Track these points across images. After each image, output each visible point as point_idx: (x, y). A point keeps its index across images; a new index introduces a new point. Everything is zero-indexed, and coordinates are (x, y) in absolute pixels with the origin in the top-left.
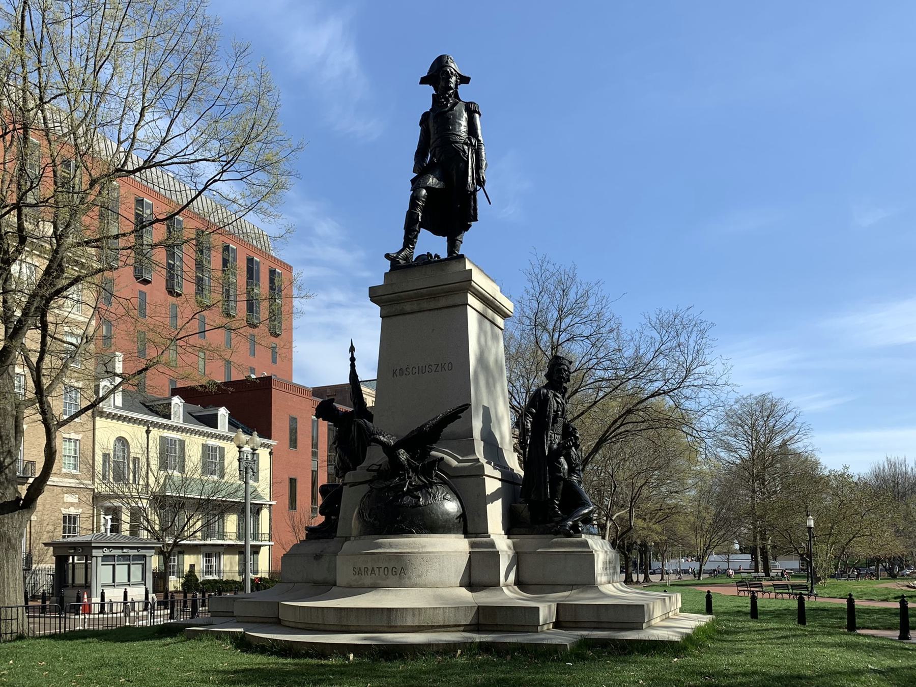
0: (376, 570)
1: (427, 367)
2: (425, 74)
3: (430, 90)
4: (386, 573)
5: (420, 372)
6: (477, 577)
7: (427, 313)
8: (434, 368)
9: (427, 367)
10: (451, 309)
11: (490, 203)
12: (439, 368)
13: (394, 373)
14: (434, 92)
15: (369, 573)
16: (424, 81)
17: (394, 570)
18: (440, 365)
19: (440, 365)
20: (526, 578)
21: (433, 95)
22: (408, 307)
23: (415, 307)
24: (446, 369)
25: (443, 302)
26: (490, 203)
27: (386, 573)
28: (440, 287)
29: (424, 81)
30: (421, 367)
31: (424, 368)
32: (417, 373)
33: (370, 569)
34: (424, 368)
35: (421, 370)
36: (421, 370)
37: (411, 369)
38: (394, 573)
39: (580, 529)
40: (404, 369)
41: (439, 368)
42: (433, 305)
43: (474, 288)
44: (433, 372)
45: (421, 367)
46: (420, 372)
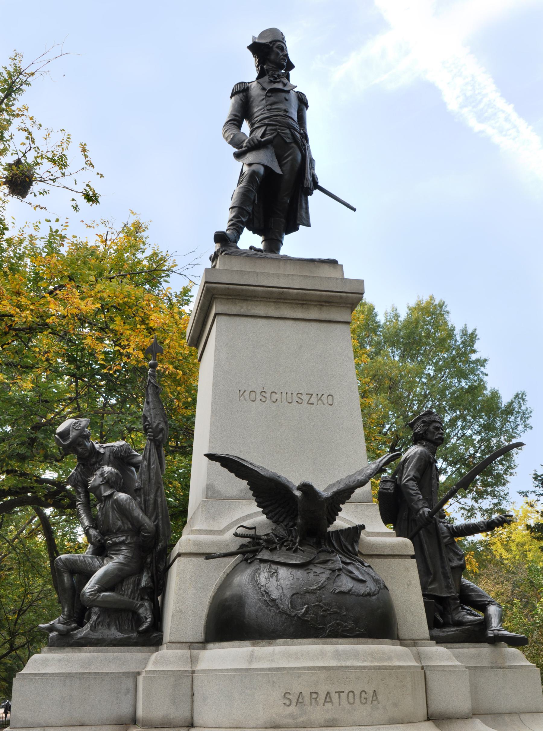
0: (335, 697)
1: (295, 395)
5: (284, 401)
7: (291, 322)
9: (295, 395)
10: (326, 325)
11: (354, 210)
12: (313, 400)
13: (242, 394)
18: (315, 395)
19: (315, 395)
22: (261, 310)
24: (325, 402)
26: (354, 210)
27: (351, 700)
30: (284, 394)
31: (289, 395)
33: (323, 696)
34: (289, 395)
37: (268, 395)
38: (364, 701)
40: (258, 392)
41: (313, 400)
42: (299, 314)
45: (284, 394)
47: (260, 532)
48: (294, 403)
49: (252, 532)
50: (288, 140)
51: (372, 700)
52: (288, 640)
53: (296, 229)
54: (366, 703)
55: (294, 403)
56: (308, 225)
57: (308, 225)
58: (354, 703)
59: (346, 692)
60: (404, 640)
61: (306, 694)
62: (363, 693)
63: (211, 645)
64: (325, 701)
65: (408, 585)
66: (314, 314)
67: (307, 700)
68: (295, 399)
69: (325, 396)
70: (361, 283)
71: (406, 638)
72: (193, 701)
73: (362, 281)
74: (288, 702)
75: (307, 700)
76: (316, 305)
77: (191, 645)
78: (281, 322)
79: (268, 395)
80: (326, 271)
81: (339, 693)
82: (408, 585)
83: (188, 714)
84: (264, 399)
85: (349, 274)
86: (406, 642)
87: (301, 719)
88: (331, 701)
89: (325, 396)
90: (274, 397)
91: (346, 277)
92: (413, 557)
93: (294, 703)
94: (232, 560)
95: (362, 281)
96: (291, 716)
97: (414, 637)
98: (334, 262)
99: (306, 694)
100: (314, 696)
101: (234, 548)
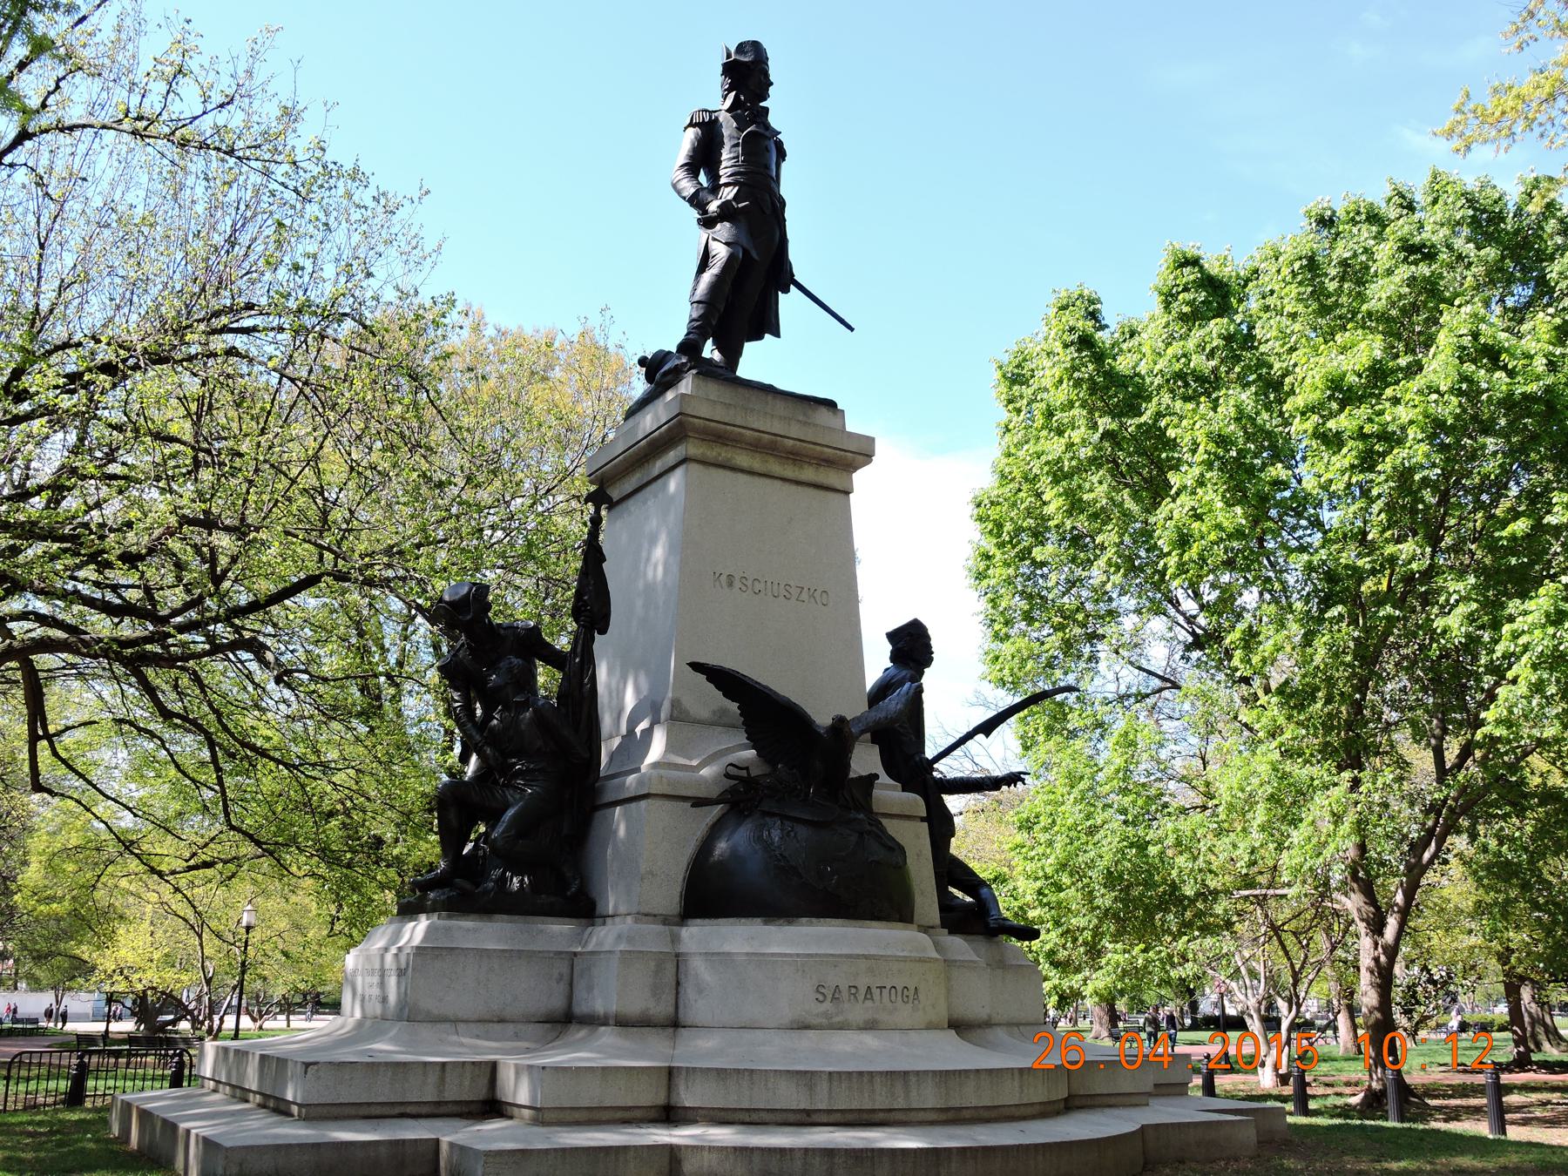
0: (876, 992)
1: (782, 586)
4: (893, 998)
7: (778, 483)
9: (782, 586)
10: (822, 493)
11: (852, 329)
12: (804, 596)
15: (861, 997)
22: (743, 459)
24: (818, 599)
25: (809, 474)
26: (852, 329)
27: (893, 998)
28: (818, 448)
30: (769, 584)
31: (776, 587)
32: (762, 594)
33: (863, 991)
34: (776, 587)
37: (749, 583)
41: (804, 596)
42: (790, 472)
44: (793, 599)
47: (754, 772)
49: (744, 773)
52: (814, 920)
53: (760, 337)
55: (782, 598)
56: (777, 334)
57: (777, 334)
61: (844, 988)
63: (690, 922)
64: (865, 998)
67: (845, 994)
69: (819, 592)
70: (871, 440)
72: (677, 993)
73: (873, 439)
74: (821, 998)
75: (845, 994)
77: (666, 920)
78: (768, 481)
79: (749, 583)
80: (823, 415)
83: (671, 1009)
84: (744, 588)
85: (853, 425)
87: (836, 1019)
89: (819, 592)
90: (758, 587)
91: (848, 429)
92: (922, 819)
93: (829, 997)
94: (716, 811)
95: (873, 439)
96: (825, 1014)
98: (830, 405)
99: (844, 988)
100: (853, 991)
101: (714, 793)
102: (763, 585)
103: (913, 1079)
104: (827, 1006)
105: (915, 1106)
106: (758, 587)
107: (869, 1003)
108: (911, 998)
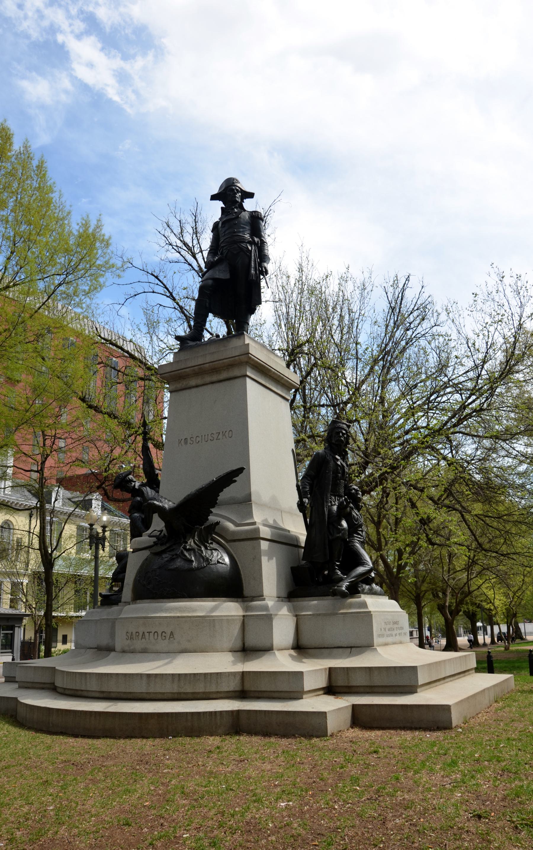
0: (147, 635)
1: (209, 435)
2: (216, 191)
3: (219, 204)
4: (156, 637)
5: (203, 441)
6: (252, 641)
7: (210, 386)
8: (215, 436)
9: (209, 435)
10: (231, 381)
12: (220, 436)
13: (180, 442)
14: (223, 206)
15: (140, 637)
16: (214, 198)
17: (164, 634)
18: (221, 433)
19: (221, 433)
20: (305, 641)
21: (222, 208)
22: (193, 382)
23: (199, 381)
27: (156, 637)
28: (221, 362)
29: (214, 198)
31: (206, 437)
34: (206, 437)
35: (203, 439)
36: (203, 439)
37: (195, 438)
39: (360, 589)
42: (215, 378)
43: (253, 360)
44: (215, 440)
46: (203, 441)
48: (209, 441)
50: (235, 252)
51: (170, 638)
54: (165, 639)
55: (209, 441)
58: (157, 639)
59: (153, 632)
60: (247, 597)
61: (134, 633)
62: (164, 634)
64: (142, 638)
65: (254, 559)
66: (208, 379)
67: (134, 636)
68: (210, 438)
69: (227, 432)
71: (249, 595)
76: (225, 370)
79: (194, 439)
81: (149, 633)
82: (254, 559)
84: (192, 443)
86: (246, 599)
88: (145, 638)
90: (198, 439)
97: (253, 595)
102: (201, 437)
103: (88, 676)
104: (129, 641)
105: (88, 689)
106: (198, 439)
107: (143, 640)
108: (168, 637)
